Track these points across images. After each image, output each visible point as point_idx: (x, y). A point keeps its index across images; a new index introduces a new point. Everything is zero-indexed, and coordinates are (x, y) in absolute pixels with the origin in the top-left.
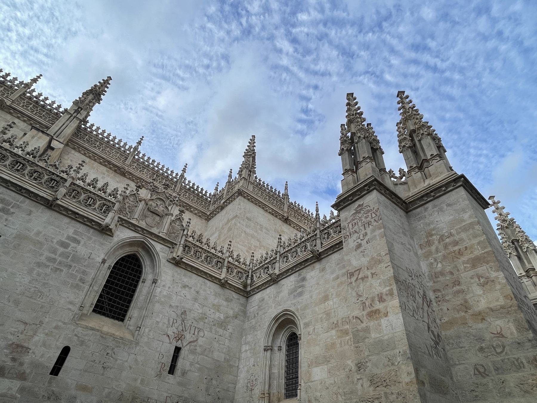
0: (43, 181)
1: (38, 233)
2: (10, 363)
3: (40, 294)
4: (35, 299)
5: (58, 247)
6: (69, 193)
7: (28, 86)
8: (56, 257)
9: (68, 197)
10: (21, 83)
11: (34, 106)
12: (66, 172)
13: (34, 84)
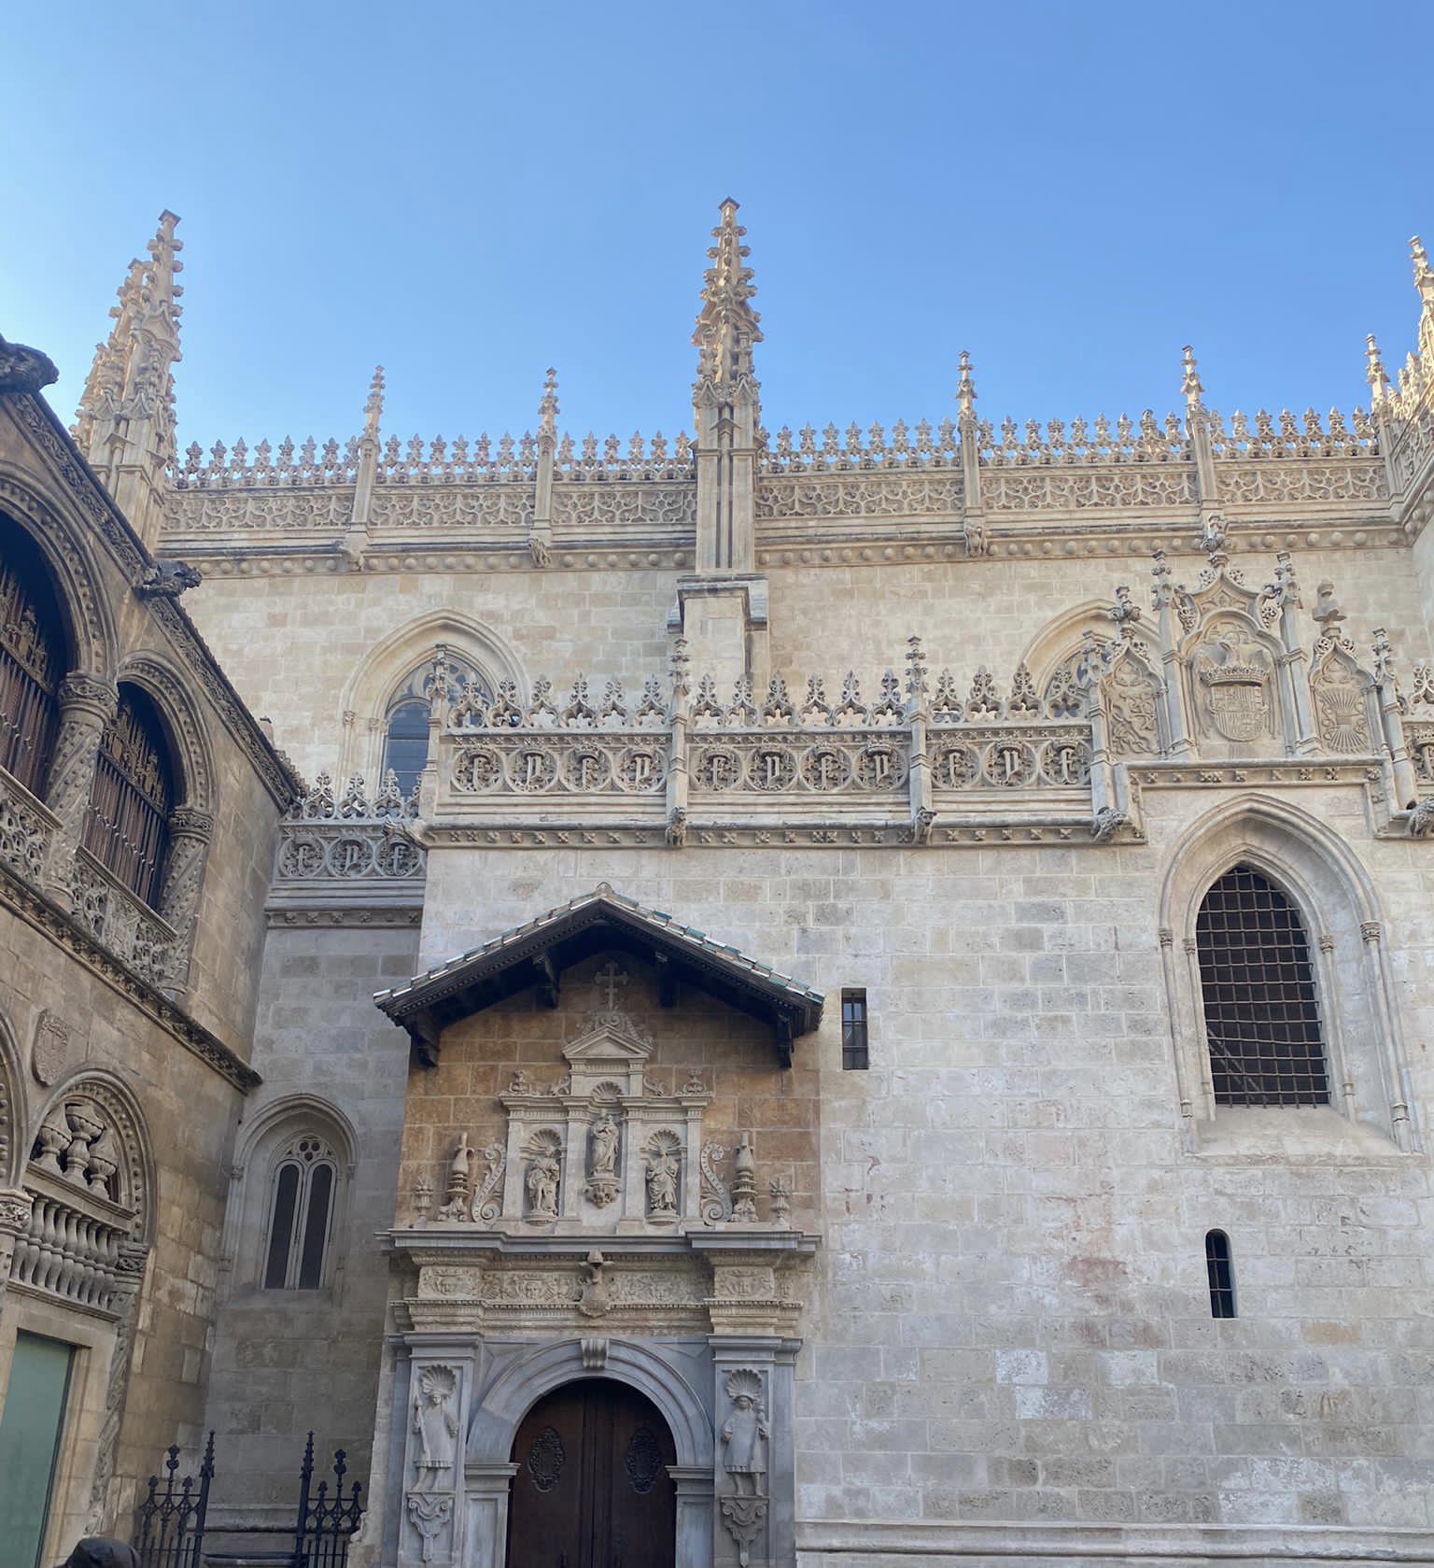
0: (854, 774)
1: (941, 939)
2: (1097, 1312)
3: (1054, 1110)
4: (1051, 1127)
5: (1014, 954)
6: (942, 775)
7: (547, 441)
8: (1028, 985)
9: (945, 787)
10: (528, 442)
11: (602, 495)
12: (890, 707)
13: (557, 420)
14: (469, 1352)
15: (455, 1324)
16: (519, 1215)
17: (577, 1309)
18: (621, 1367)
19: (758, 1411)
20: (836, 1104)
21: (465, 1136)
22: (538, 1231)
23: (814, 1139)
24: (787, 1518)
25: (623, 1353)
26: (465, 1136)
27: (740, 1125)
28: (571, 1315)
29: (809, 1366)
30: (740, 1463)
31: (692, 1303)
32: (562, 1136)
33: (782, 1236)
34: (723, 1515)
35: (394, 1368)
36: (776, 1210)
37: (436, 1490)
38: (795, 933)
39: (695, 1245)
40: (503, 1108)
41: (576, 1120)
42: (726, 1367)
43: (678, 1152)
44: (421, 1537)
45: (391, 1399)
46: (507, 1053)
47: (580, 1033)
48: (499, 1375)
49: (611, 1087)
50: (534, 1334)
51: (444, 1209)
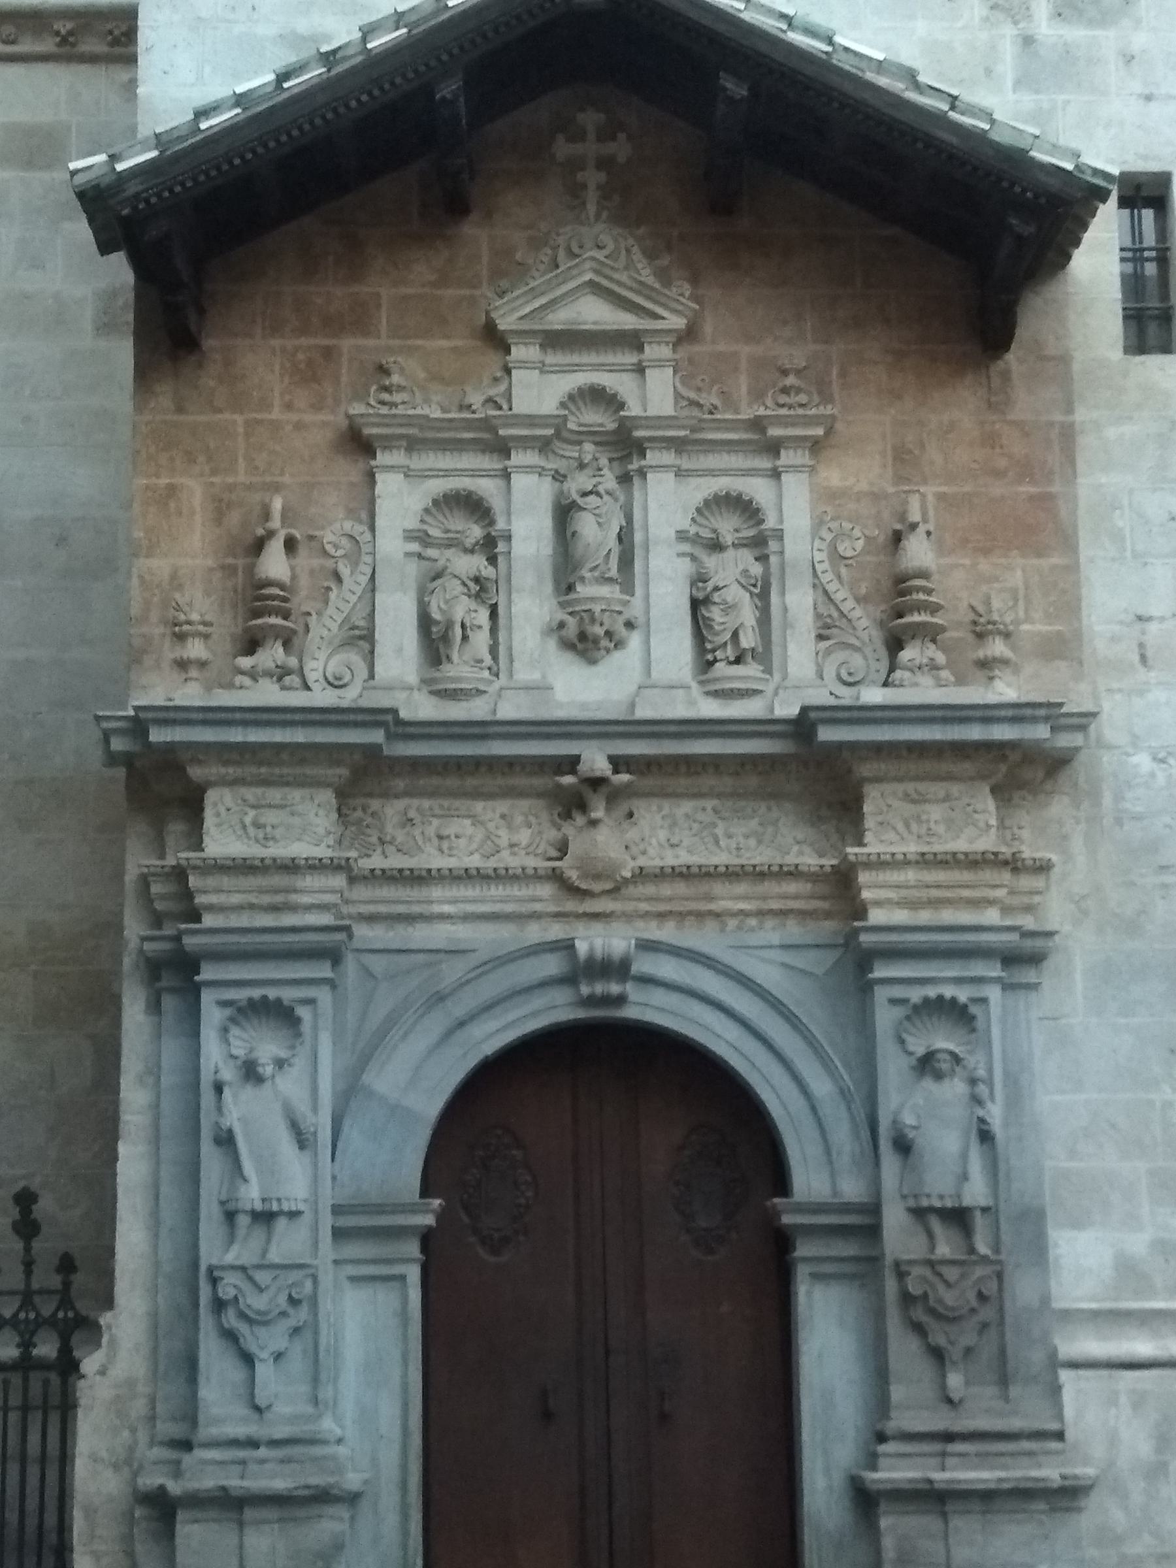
14: (324, 970)
15: (293, 908)
16: (412, 678)
17: (556, 877)
18: (659, 997)
19: (973, 1082)
20: (1111, 433)
21: (277, 504)
22: (457, 711)
23: (1063, 513)
25: (667, 968)
26: (277, 504)
27: (899, 479)
28: (545, 890)
29: (1070, 988)
30: (938, 1187)
31: (810, 860)
32: (497, 504)
33: (1018, 713)
34: (907, 1299)
35: (155, 1007)
36: (985, 664)
37: (274, 1256)
38: (1008, 50)
39: (826, 734)
40: (359, 444)
41: (528, 469)
42: (898, 992)
43: (759, 544)
44: (248, 1360)
45: (154, 1071)
46: (359, 319)
47: (523, 271)
48: (391, 1021)
49: (597, 396)
50: (462, 933)
51: (245, 662)
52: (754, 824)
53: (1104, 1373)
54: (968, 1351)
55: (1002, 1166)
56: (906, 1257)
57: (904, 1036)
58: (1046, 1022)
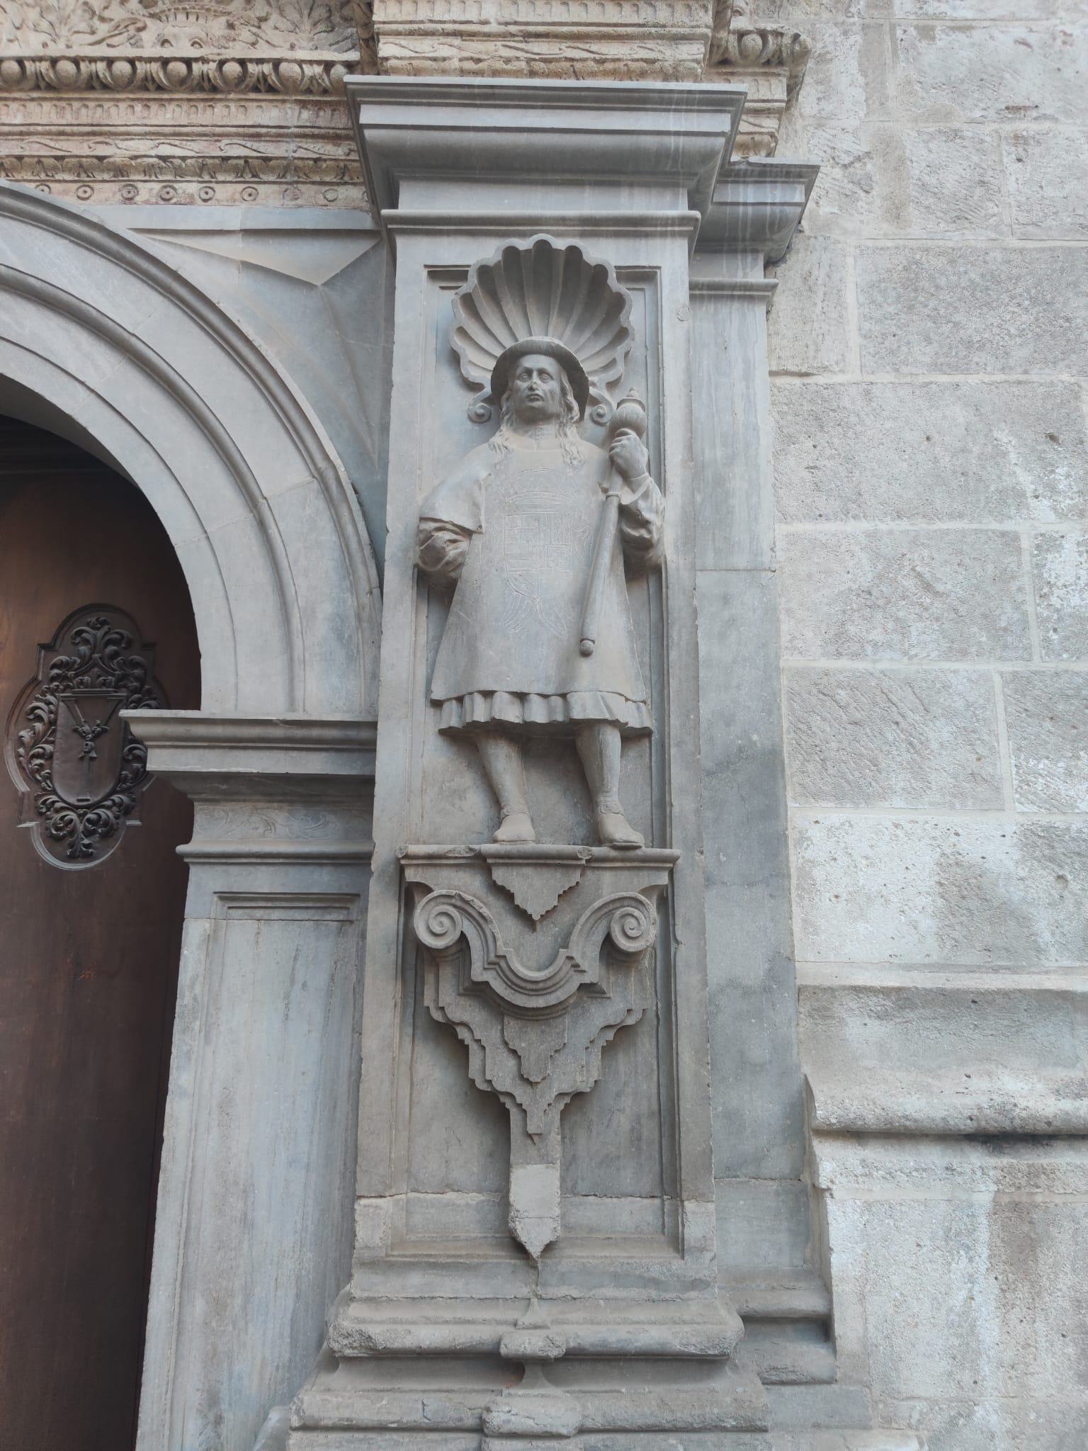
24: (754, 970)
52: (217, 27)
53: (934, 1156)
54: (576, 1101)
55: (678, 634)
56: (414, 849)
57: (459, 343)
58: (781, 381)
